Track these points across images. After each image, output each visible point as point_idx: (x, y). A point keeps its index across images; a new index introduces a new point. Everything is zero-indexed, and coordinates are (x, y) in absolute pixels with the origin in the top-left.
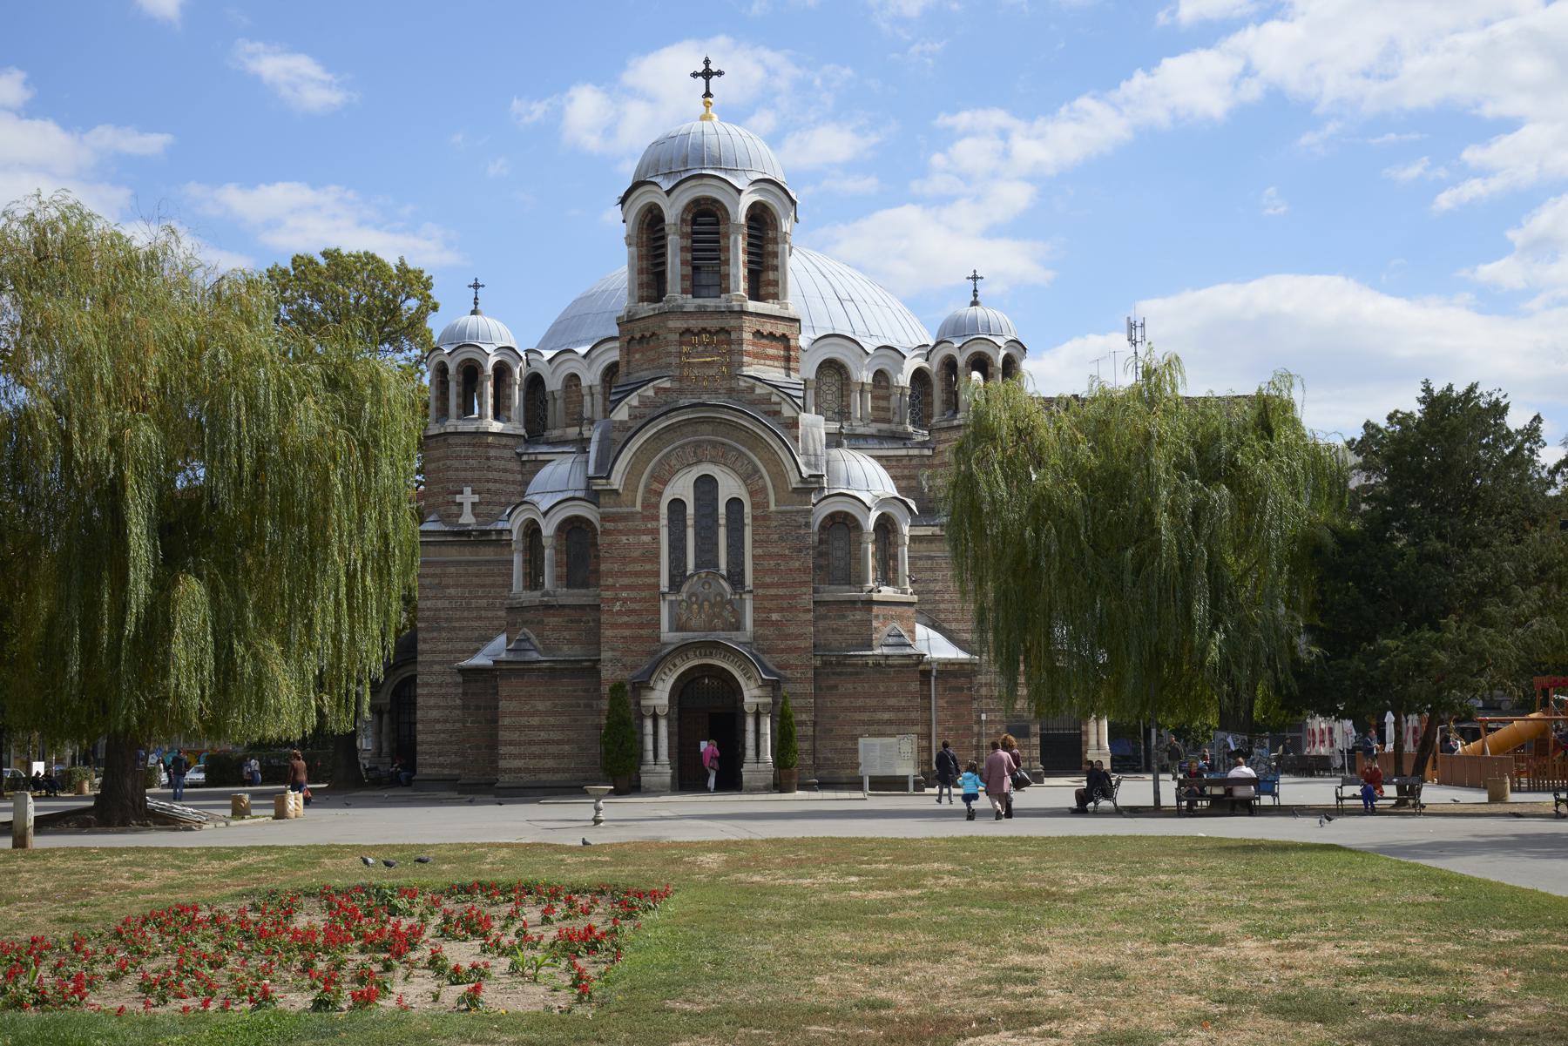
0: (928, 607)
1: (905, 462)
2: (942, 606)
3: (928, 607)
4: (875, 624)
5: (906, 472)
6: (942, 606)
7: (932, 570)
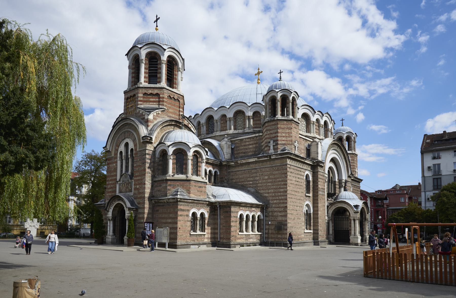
0: (255, 185)
1: (255, 139)
2: (259, 185)
3: (255, 185)
4: (168, 188)
5: (255, 142)
6: (259, 185)
7: (256, 173)
